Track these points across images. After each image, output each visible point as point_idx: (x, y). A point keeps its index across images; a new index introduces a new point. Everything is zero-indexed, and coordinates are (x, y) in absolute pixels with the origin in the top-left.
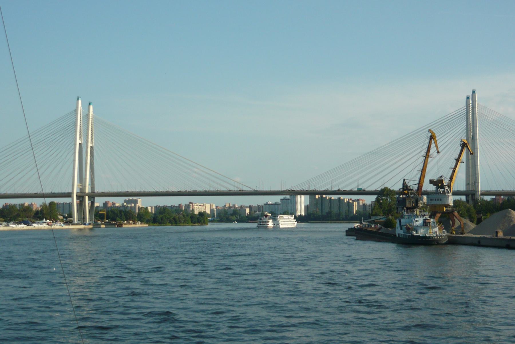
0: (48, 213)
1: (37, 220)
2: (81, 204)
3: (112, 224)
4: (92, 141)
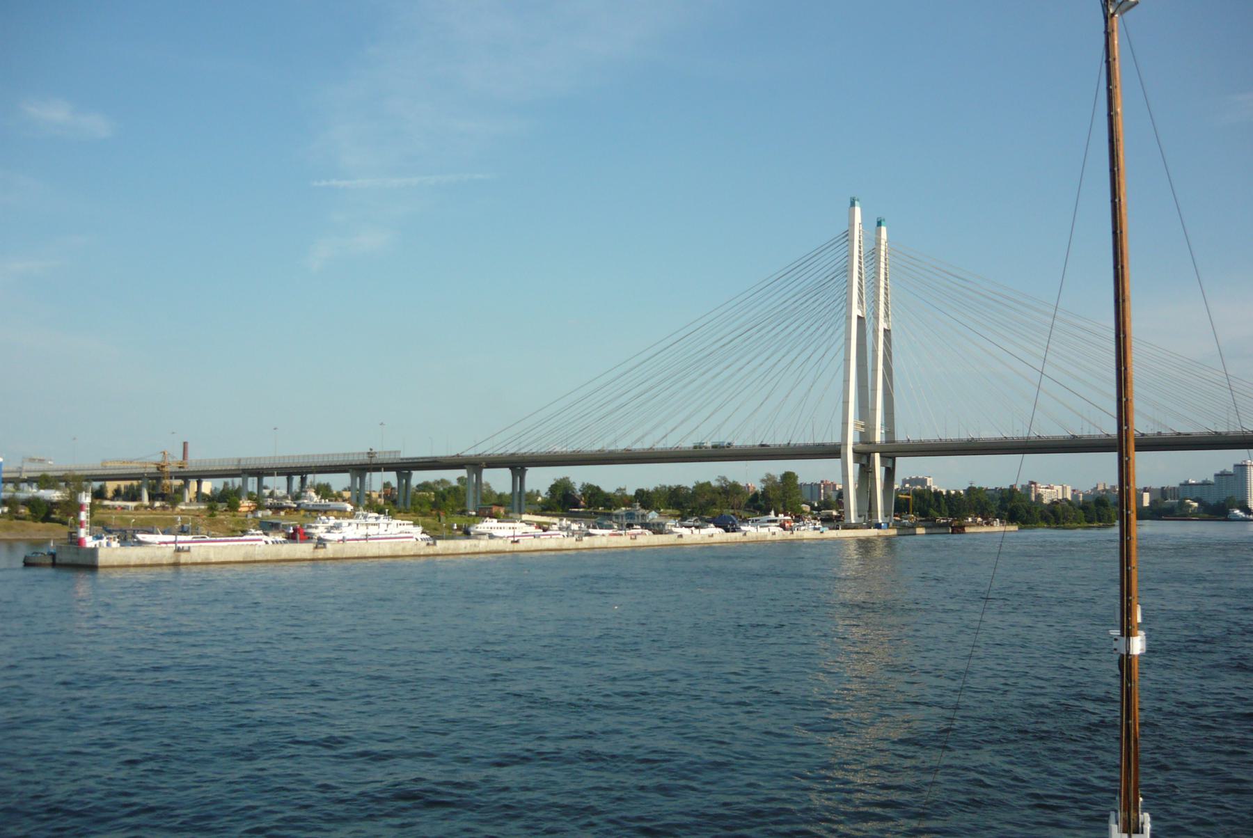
0: (778, 499)
1: (754, 513)
2: (866, 472)
3: (942, 526)
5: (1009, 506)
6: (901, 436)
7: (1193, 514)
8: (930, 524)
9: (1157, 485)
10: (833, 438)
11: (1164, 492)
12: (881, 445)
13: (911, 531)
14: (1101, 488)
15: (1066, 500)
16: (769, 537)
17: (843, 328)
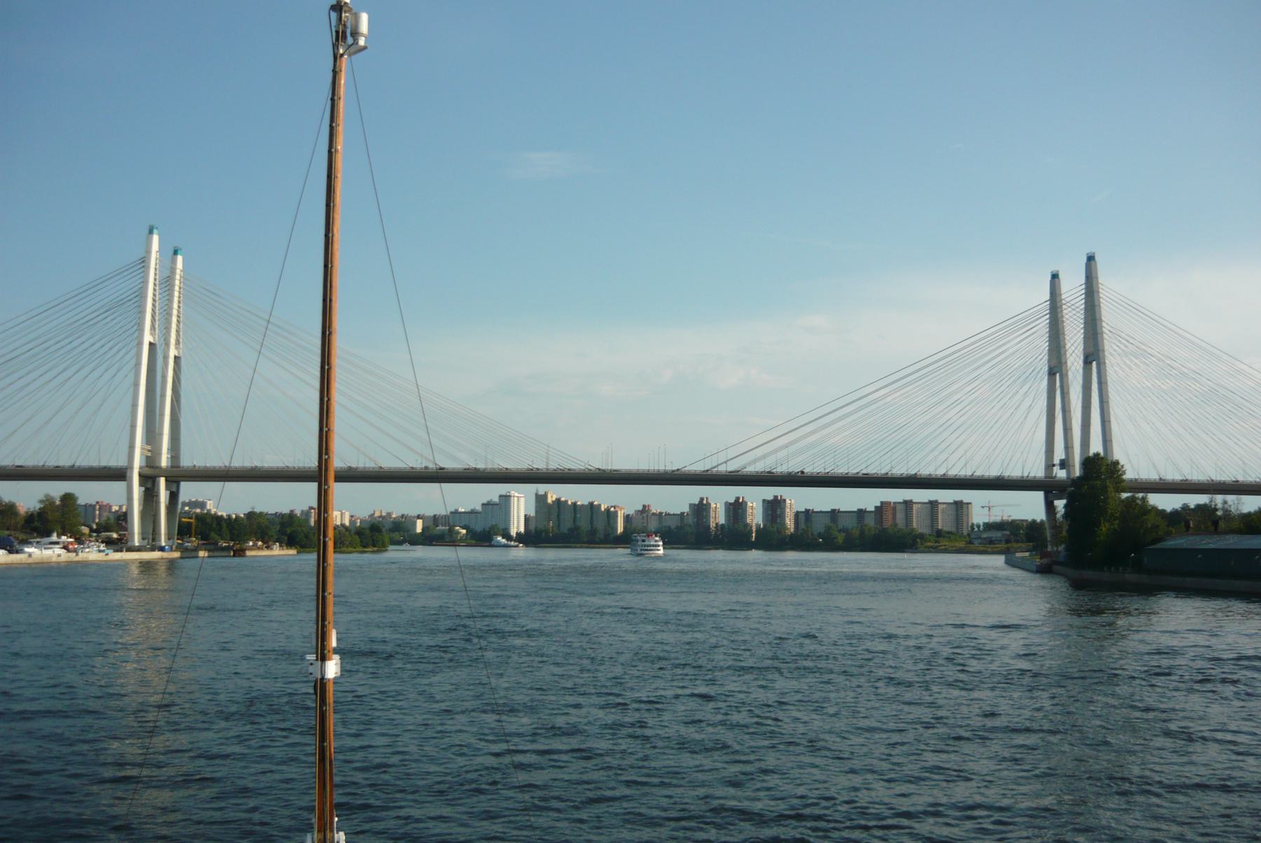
2: (150, 495)
3: (223, 549)
4: (178, 342)
5: (289, 531)
6: (186, 462)
7: (461, 540)
8: (212, 547)
9: (430, 513)
10: (117, 461)
11: (436, 519)
12: (166, 470)
13: (193, 554)
14: (377, 514)
15: (343, 525)
16: (54, 559)
17: (133, 352)
